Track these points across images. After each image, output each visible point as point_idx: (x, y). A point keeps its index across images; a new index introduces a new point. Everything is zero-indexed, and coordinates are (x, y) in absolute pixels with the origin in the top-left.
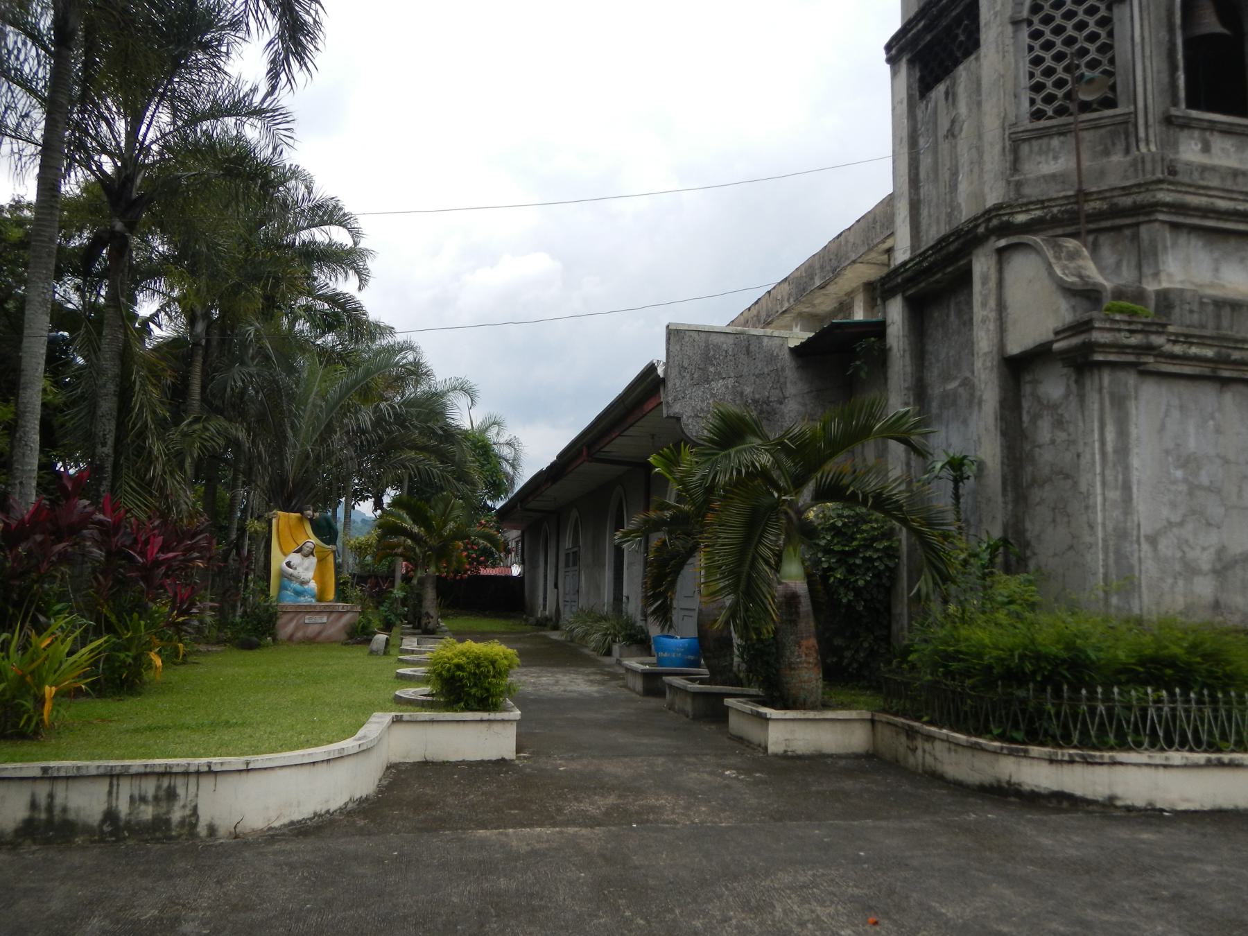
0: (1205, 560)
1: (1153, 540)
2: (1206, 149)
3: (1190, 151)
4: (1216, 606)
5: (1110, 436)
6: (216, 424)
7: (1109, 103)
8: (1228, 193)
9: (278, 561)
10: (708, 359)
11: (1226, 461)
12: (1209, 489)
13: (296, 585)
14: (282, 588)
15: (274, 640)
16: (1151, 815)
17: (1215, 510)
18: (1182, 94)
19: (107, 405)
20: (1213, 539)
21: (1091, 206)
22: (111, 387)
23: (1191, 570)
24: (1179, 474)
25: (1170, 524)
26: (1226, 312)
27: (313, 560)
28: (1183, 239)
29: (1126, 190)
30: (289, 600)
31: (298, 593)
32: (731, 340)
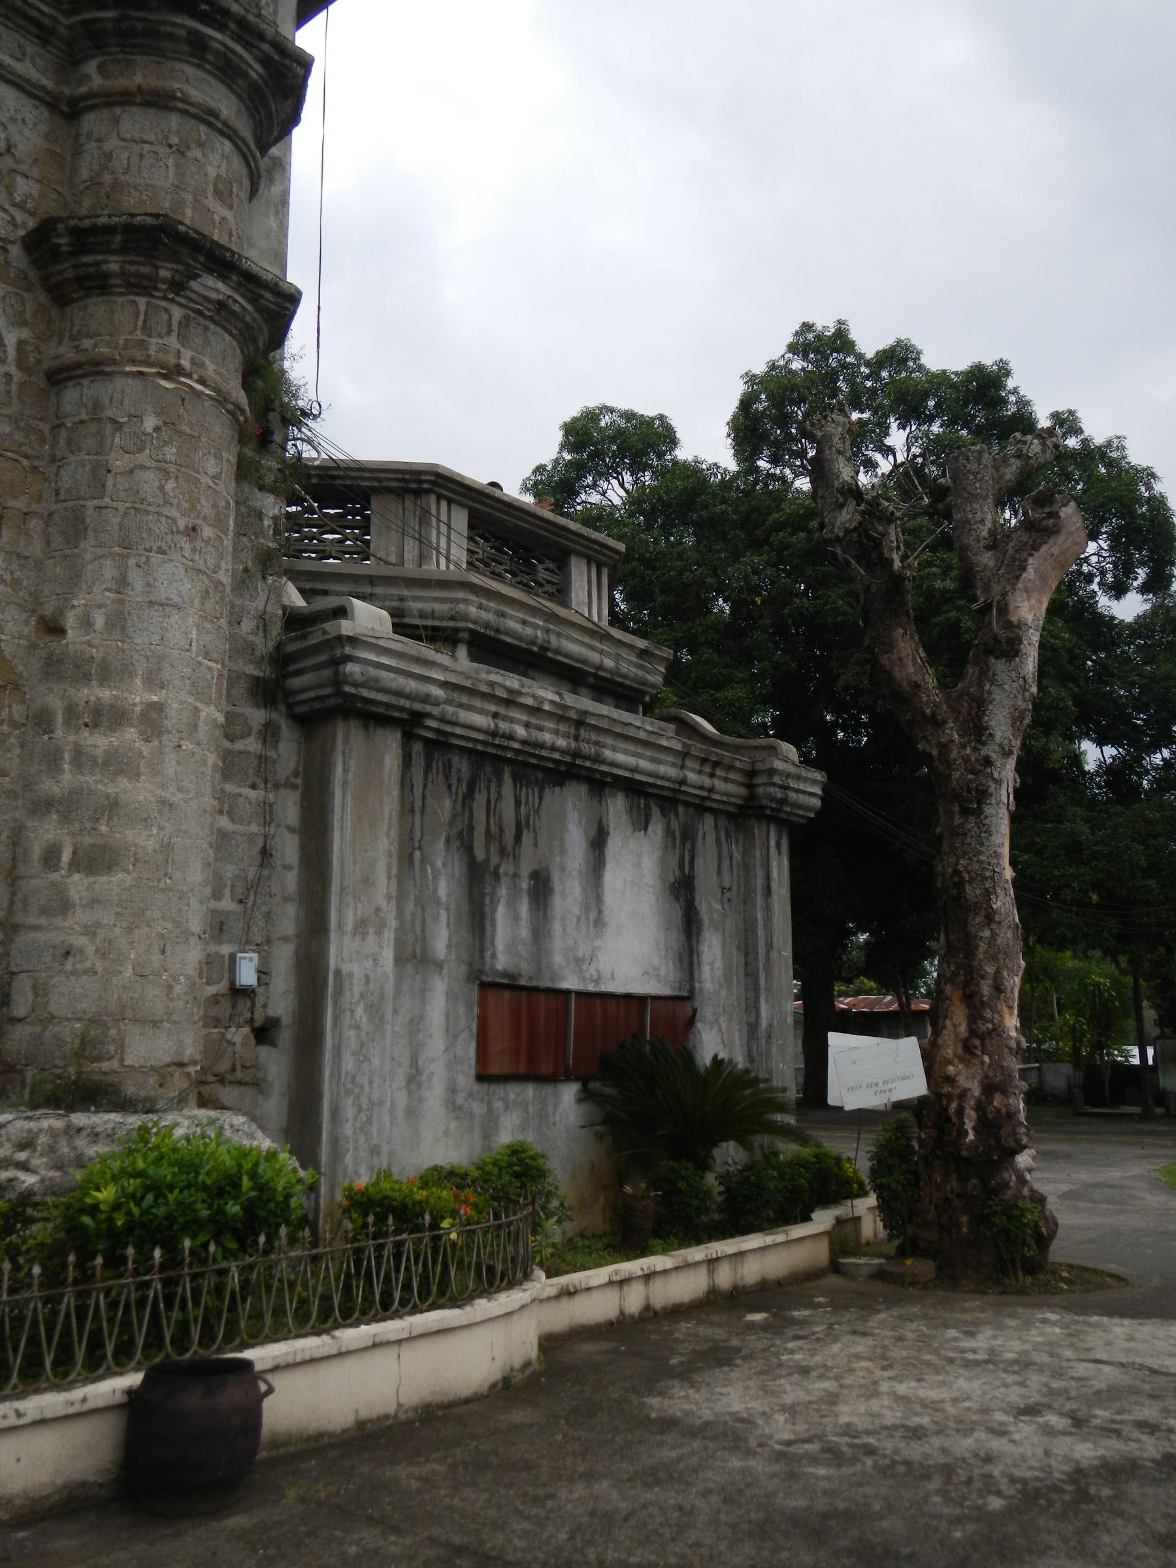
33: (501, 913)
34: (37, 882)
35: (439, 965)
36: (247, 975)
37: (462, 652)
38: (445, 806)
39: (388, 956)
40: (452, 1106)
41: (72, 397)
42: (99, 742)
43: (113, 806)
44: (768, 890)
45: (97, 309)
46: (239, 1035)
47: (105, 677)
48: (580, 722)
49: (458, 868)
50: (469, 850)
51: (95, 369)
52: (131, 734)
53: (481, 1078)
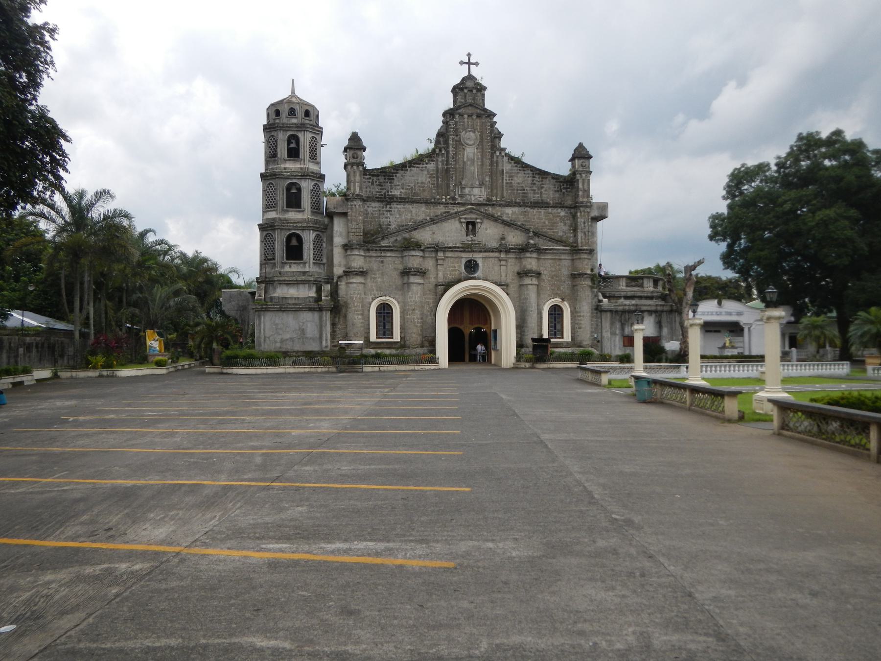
0: (278, 341)
1: (269, 338)
2: (290, 267)
3: (287, 268)
4: (280, 348)
5: (257, 322)
6: (132, 309)
7: (274, 259)
8: (288, 277)
9: (148, 343)
10: (231, 297)
11: (283, 324)
12: (280, 329)
13: (153, 349)
14: (150, 349)
15: (148, 362)
16: (237, 374)
17: (281, 332)
18: (285, 258)
19: (103, 316)
20: (280, 337)
21: (267, 280)
22: (103, 312)
23: (276, 342)
24: (274, 327)
25: (272, 335)
26: (284, 299)
27: (158, 342)
28: (282, 285)
29: (271, 277)
30: (152, 352)
31: (154, 351)
32: (236, 293)
33: (626, 329)
34: (576, 330)
35: (617, 335)
36: (596, 336)
37: (622, 298)
38: (618, 317)
39: (609, 334)
40: (620, 348)
41: (575, 288)
42: (579, 318)
43: (581, 324)
44: (675, 321)
45: (576, 279)
46: (595, 342)
47: (580, 312)
48: (637, 305)
49: (620, 324)
50: (621, 322)
51: (576, 286)
52: (582, 318)
53: (624, 346)
